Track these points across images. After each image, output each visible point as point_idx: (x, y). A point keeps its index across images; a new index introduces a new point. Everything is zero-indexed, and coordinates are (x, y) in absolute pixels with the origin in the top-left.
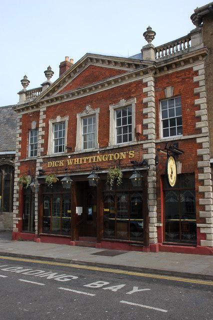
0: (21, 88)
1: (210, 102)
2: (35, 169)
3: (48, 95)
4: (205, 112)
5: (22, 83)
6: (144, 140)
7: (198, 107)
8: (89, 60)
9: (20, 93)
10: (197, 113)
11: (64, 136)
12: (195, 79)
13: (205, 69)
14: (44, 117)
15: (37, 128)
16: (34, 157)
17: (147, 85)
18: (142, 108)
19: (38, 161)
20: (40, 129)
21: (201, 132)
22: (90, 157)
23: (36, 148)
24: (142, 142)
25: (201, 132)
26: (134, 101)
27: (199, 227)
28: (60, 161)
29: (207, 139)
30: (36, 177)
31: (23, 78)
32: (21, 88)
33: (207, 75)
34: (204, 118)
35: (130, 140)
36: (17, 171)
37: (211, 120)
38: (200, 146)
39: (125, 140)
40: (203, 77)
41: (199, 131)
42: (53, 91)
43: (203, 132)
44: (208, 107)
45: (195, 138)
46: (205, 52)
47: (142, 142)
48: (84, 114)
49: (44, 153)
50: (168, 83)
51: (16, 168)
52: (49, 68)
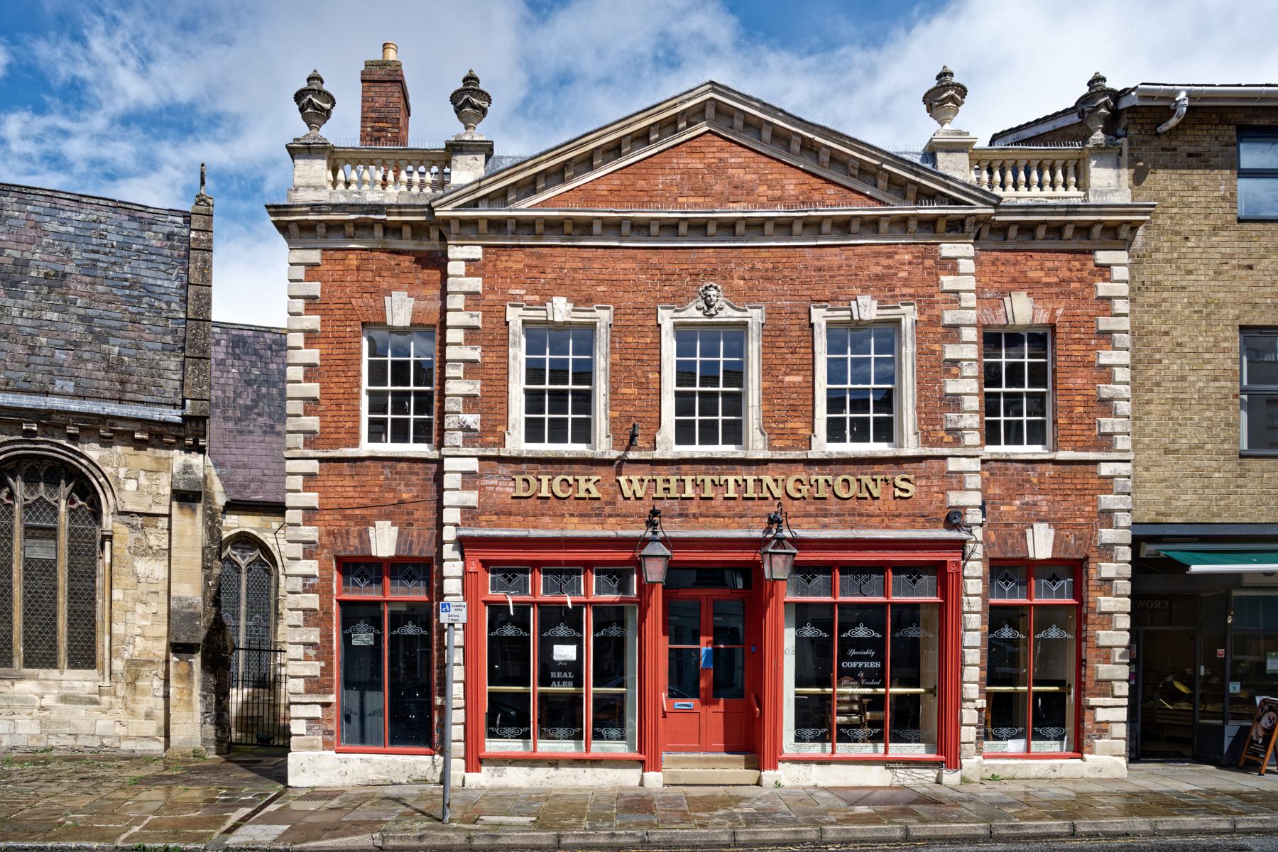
1: (1140, 367)
3: (500, 197)
4: (1125, 390)
7: (1107, 374)
8: (710, 112)
10: (1106, 390)
21: (1110, 447)
25: (1110, 447)
27: (1093, 708)
28: (582, 479)
29: (1125, 468)
33: (1137, 288)
34: (1124, 407)
35: (885, 431)
37: (1139, 419)
38: (1107, 484)
41: (1105, 441)
43: (1119, 447)
44: (1133, 379)
45: (1096, 462)
48: (693, 313)
50: (1014, 280)
52: (470, 79)
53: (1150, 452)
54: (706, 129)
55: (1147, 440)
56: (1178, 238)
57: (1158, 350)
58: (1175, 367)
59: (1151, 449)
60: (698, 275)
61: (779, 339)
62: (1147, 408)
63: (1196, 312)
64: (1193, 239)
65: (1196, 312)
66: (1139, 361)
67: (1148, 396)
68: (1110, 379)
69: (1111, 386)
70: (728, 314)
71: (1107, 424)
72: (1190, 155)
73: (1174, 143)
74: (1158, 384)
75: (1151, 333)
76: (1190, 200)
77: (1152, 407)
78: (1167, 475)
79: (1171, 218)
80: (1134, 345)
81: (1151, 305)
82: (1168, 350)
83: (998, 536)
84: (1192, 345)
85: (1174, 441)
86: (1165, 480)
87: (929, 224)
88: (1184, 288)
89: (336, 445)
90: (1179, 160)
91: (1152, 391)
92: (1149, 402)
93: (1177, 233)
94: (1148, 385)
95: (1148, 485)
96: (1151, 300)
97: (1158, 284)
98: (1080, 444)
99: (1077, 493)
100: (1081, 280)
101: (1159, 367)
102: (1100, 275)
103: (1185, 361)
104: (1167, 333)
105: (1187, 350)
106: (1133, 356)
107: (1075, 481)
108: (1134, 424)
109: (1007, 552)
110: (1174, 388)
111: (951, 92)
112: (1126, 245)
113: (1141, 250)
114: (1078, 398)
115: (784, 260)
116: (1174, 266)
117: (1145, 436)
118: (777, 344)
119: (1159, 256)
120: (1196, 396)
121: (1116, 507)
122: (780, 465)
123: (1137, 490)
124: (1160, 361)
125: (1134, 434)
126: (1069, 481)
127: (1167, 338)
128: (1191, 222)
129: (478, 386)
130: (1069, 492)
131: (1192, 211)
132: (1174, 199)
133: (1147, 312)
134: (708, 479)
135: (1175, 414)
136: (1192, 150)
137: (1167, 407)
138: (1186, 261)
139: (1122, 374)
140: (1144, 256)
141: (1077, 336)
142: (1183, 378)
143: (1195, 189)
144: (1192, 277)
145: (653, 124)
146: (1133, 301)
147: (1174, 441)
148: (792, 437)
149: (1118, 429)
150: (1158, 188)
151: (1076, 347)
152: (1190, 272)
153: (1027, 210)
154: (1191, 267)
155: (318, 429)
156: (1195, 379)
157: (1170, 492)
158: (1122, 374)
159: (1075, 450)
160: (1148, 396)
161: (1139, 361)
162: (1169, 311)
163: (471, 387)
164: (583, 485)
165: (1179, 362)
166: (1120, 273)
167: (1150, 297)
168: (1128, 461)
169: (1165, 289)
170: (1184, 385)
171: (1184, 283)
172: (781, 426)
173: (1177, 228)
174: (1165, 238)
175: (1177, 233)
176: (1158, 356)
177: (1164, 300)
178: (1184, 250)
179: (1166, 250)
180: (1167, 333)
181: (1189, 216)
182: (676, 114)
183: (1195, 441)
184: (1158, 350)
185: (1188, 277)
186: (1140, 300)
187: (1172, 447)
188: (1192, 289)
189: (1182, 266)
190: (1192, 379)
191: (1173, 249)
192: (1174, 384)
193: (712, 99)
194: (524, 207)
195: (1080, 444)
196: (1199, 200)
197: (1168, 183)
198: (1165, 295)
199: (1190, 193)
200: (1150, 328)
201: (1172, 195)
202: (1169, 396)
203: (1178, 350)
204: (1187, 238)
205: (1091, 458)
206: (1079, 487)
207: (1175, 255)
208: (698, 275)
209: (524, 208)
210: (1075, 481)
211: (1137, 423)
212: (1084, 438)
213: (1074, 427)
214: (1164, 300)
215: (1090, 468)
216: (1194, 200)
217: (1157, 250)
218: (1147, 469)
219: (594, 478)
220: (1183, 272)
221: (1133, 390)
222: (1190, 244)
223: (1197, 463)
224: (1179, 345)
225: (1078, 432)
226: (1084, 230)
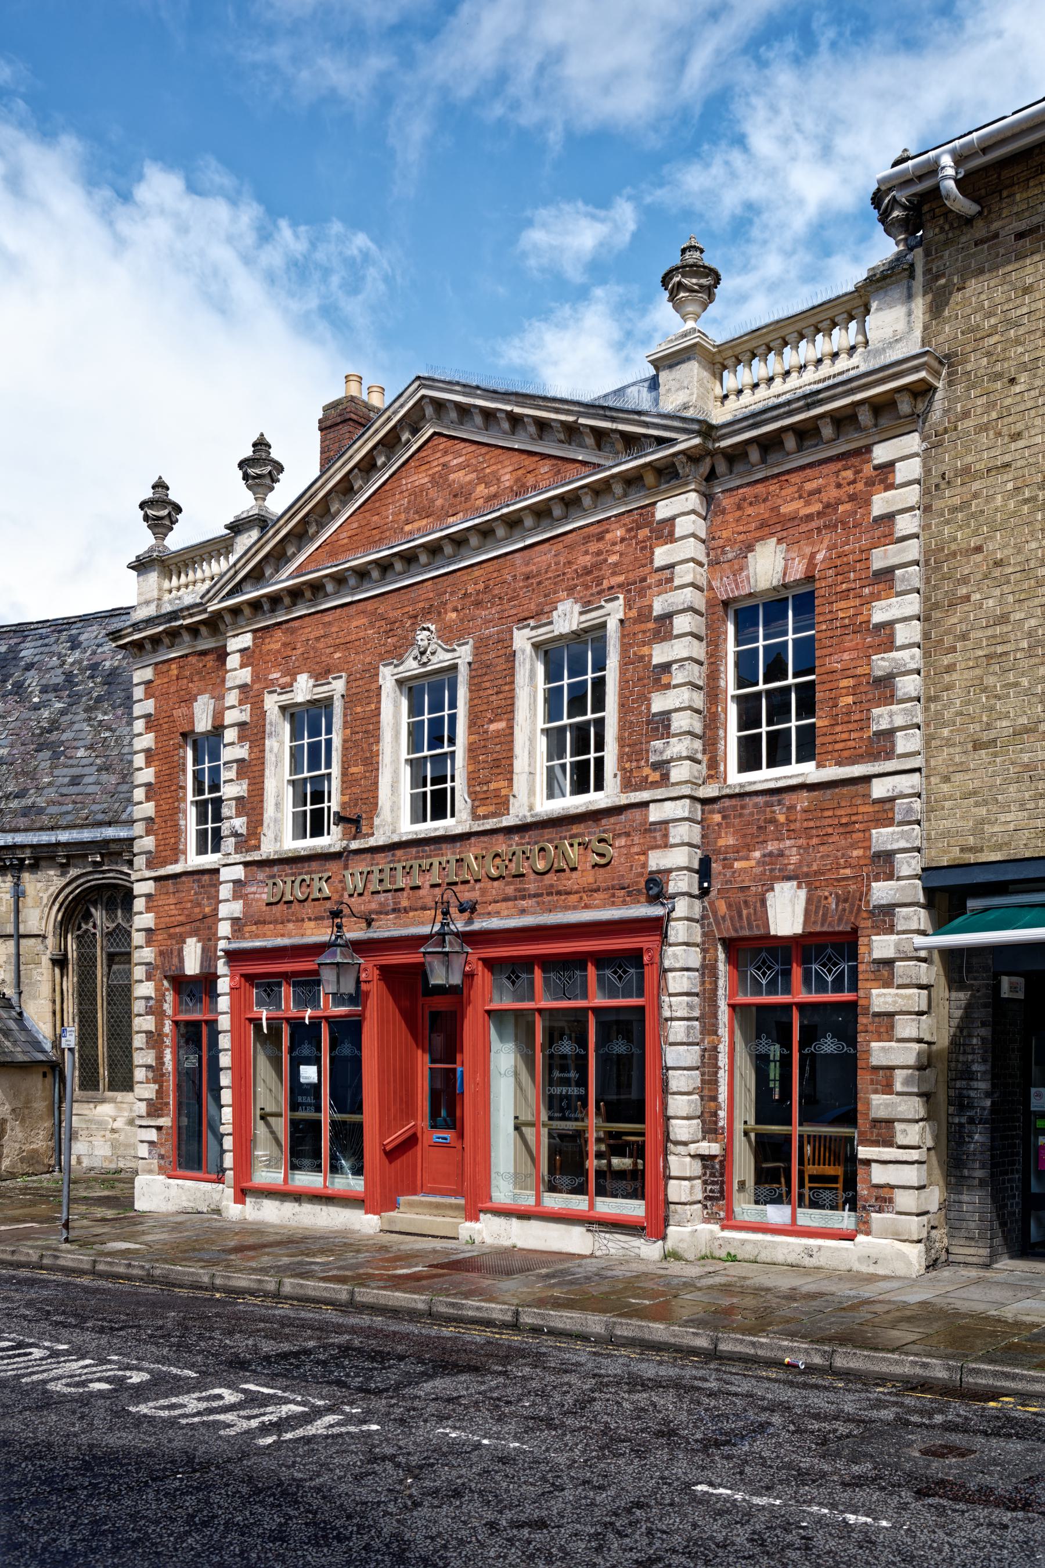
0: (144, 540)
1: (936, 615)
2: (216, 909)
4: (912, 658)
5: (146, 518)
6: (655, 785)
9: (141, 566)
10: (882, 663)
11: (328, 765)
12: (881, 503)
13: (926, 456)
14: (245, 675)
15: (218, 729)
16: (210, 860)
17: (672, 533)
18: (649, 643)
19: (226, 874)
20: (230, 735)
21: (889, 754)
22: (435, 861)
23: (218, 818)
24: (644, 796)
25: (889, 754)
26: (614, 612)
28: (316, 877)
30: (222, 944)
31: (148, 494)
32: (144, 540)
34: (908, 685)
36: (144, 920)
37: (930, 699)
39: (580, 787)
40: (912, 495)
42: (278, 557)
43: (900, 749)
44: (926, 635)
45: (867, 779)
46: (923, 374)
47: (644, 796)
49: (248, 840)
51: (139, 904)
53: (952, 750)
54: (431, 431)
55: (946, 732)
56: (999, 385)
57: (965, 580)
58: (991, 602)
59: (953, 745)
60: (416, 617)
61: (486, 678)
62: (947, 678)
63: (1026, 501)
64: (1023, 378)
65: (1026, 501)
66: (936, 606)
67: (946, 660)
68: (889, 645)
69: (894, 654)
70: (441, 659)
71: (883, 717)
72: (1020, 236)
73: (995, 226)
74: (964, 637)
75: (954, 554)
76: (1019, 312)
77: (955, 676)
78: (977, 783)
79: (989, 354)
80: (928, 581)
81: (954, 510)
82: (979, 576)
83: (729, 906)
84: (1020, 558)
85: (989, 727)
86: (975, 793)
87: (632, 481)
88: (1007, 465)
89: (164, 863)
90: (1002, 251)
91: (953, 649)
92: (950, 669)
93: (997, 376)
94: (948, 641)
95: (948, 804)
96: (957, 501)
97: (966, 470)
98: (846, 754)
99: (842, 830)
100: (852, 498)
101: (967, 607)
102: (882, 481)
103: (1006, 589)
104: (979, 549)
105: (1010, 570)
106: (926, 599)
107: (839, 812)
108: (927, 709)
109: (742, 928)
110: (988, 638)
111: (676, 279)
112: (914, 421)
113: (941, 423)
114: (844, 683)
115: (495, 575)
116: (991, 433)
117: (944, 725)
118: (484, 685)
119: (969, 423)
120: (1025, 644)
121: (895, 846)
122: (482, 839)
123: (932, 815)
124: (967, 598)
125: (928, 725)
126: (830, 813)
127: (978, 558)
128: (1020, 349)
129: (245, 787)
130: (830, 830)
131: (1022, 330)
132: (993, 321)
133: (947, 522)
134: (415, 864)
135: (990, 680)
136: (1022, 226)
137: (978, 672)
138: (1010, 419)
139: (907, 633)
140: (946, 431)
141: (844, 586)
142: (1003, 619)
143: (1027, 290)
144: (1021, 444)
145: (374, 448)
146: (927, 509)
147: (989, 727)
148: (495, 801)
149: (899, 721)
150: (969, 310)
151: (843, 604)
152: (1017, 436)
153: (755, 418)
154: (1020, 426)
155: (153, 849)
156: (1022, 615)
157: (983, 811)
158: (907, 633)
159: (839, 764)
160: (946, 660)
161: (936, 606)
162: (982, 512)
163: (238, 788)
164: (316, 884)
165: (997, 592)
166: (908, 470)
167: (951, 497)
168: (918, 770)
169: (977, 476)
170: (1006, 628)
171: (1007, 458)
172: (485, 788)
173: (998, 367)
174: (978, 392)
175: (997, 376)
176: (963, 591)
177: (976, 496)
178: (1009, 401)
179: (979, 411)
180: (979, 549)
181: (1018, 342)
182: (394, 428)
183: (1024, 720)
184: (965, 580)
185: (1013, 446)
186: (937, 505)
187: (985, 736)
188: (1019, 463)
189: (1005, 431)
190: (1019, 616)
191: (991, 406)
192: (989, 632)
193: (423, 397)
194: (284, 577)
195: (846, 754)
196: (1034, 307)
197: (983, 297)
198: (976, 486)
199: (1018, 302)
200: (954, 547)
201: (990, 315)
202: (980, 653)
203: (997, 572)
204: (1012, 381)
205: (857, 774)
206: (844, 821)
207: (994, 415)
208: (416, 617)
209: (283, 580)
210: (839, 812)
211: (932, 706)
212: (851, 744)
213: (838, 729)
214: (976, 496)
215: (860, 788)
216: (1025, 310)
217: (966, 414)
218: (946, 779)
219: (326, 875)
220: (1006, 439)
221: (927, 655)
222: (1018, 389)
223: (1026, 758)
224: (998, 564)
225: (845, 736)
226: (844, 420)
